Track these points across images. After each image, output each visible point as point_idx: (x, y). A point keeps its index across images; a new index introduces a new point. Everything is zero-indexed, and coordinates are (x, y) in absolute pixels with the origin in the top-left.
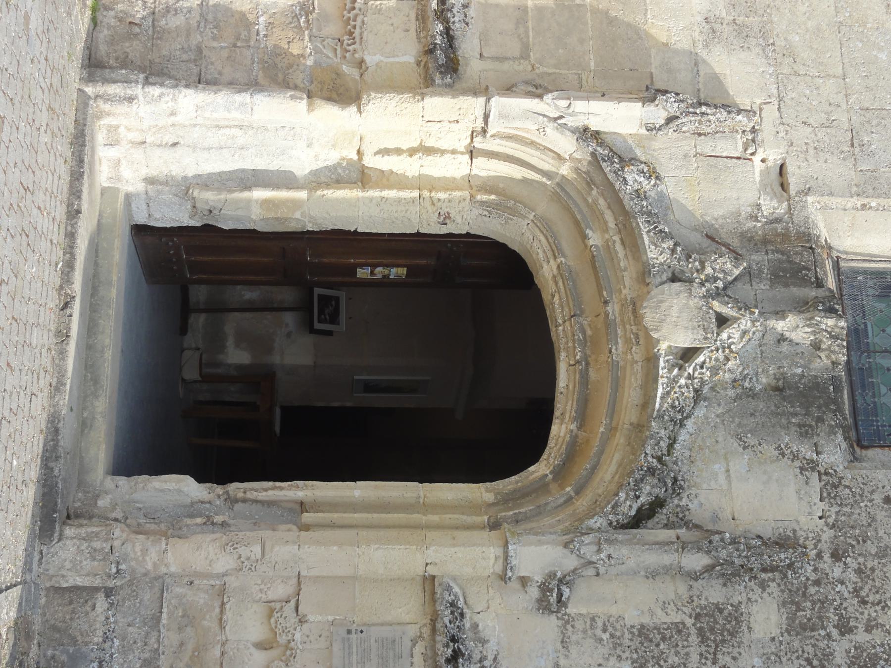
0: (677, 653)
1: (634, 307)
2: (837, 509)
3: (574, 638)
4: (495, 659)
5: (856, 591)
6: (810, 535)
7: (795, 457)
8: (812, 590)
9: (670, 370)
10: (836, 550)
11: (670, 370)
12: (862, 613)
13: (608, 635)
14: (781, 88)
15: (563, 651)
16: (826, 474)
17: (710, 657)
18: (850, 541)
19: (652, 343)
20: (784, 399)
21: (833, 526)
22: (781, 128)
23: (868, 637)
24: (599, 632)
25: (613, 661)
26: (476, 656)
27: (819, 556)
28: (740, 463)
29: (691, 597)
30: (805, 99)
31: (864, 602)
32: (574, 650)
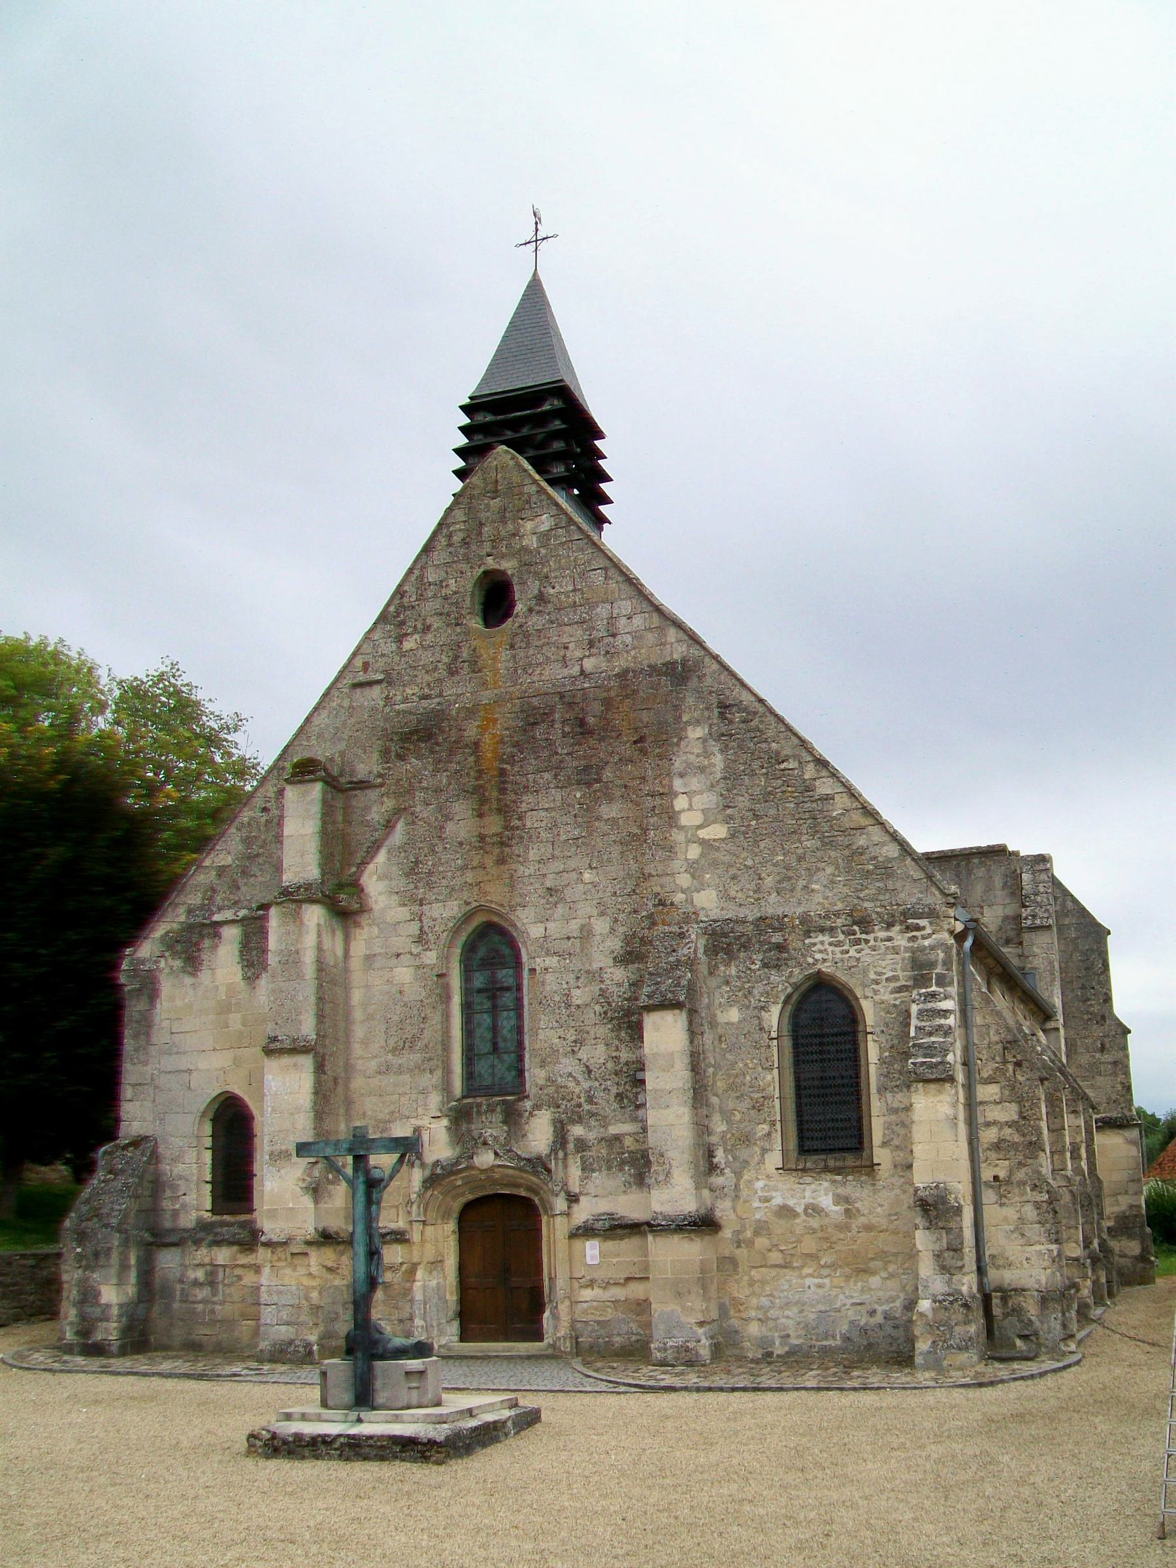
1: (482, 1171)
5: (569, 1101)
19: (493, 1166)
28: (530, 1136)
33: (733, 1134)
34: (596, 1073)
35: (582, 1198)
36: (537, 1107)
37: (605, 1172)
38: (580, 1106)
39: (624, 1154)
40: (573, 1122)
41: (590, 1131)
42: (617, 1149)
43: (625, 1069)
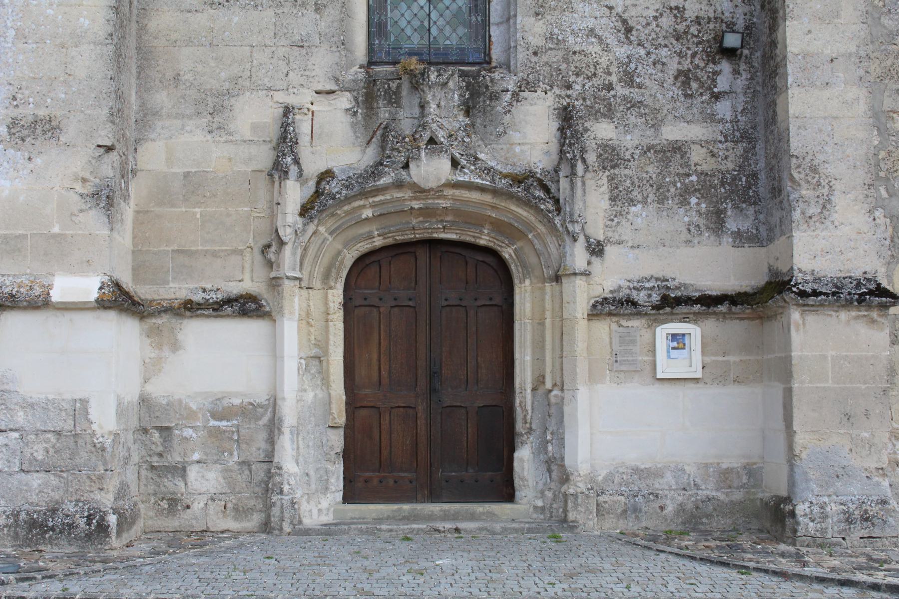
0: (625, 181)
1: (419, 191)
2: (541, 83)
3: (617, 237)
4: (629, 281)
6: (557, 100)
7: (510, 104)
8: (588, 103)
9: (465, 174)
10: (565, 87)
11: (465, 174)
12: (601, 76)
13: (615, 219)
14: (261, 87)
15: (624, 244)
16: (520, 87)
17: (626, 163)
18: (560, 78)
20: (474, 107)
21: (551, 86)
22: (291, 90)
23: (614, 75)
24: (614, 224)
25: (629, 217)
26: (628, 291)
27: (569, 96)
28: (515, 136)
29: (593, 171)
30: (269, 73)
32: (624, 238)
33: (889, 153)
34: (640, 32)
35: (608, 249)
36: (528, 85)
37: (653, 207)
38: (609, 87)
39: (689, 175)
40: (596, 115)
41: (626, 132)
42: (675, 166)
43: (693, 30)
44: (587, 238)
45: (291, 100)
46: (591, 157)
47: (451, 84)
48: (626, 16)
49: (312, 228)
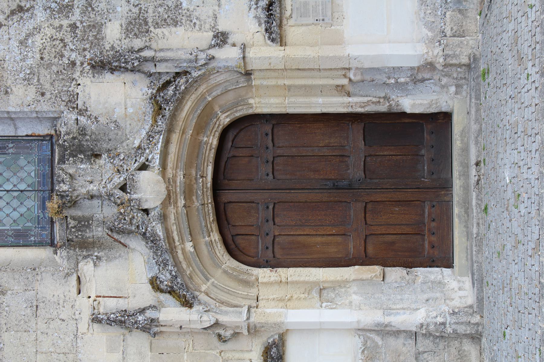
0: (159, 13)
1: (168, 200)
2: (70, 89)
3: (210, 20)
4: (250, 9)
6: (86, 75)
7: (89, 117)
8: (88, 46)
9: (153, 158)
10: (73, 67)
11: (153, 158)
12: (63, 34)
13: (193, 22)
14: (74, 344)
15: (216, 13)
16: (74, 108)
17: (143, 11)
18: (65, 72)
20: (92, 150)
21: (73, 80)
22: (77, 317)
23: (62, 23)
24: (198, 23)
25: (191, 9)
26: (260, 10)
27: (82, 64)
28: (119, 113)
29: (150, 41)
30: (61, 337)
31: (62, 40)
32: (211, 13)
35: (221, 28)
40: (99, 39)
44: (211, 47)
45: (86, 316)
46: (138, 43)
47: (71, 171)
48: (8, 12)
49: (202, 297)
